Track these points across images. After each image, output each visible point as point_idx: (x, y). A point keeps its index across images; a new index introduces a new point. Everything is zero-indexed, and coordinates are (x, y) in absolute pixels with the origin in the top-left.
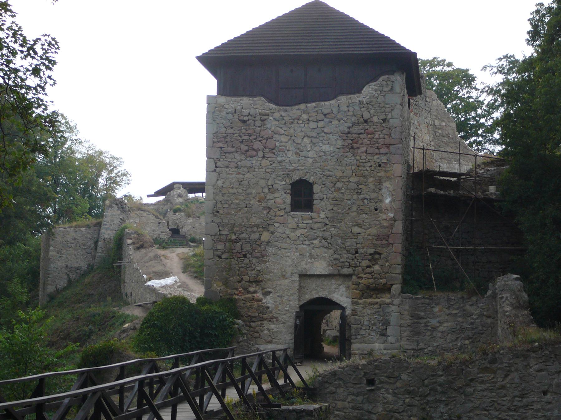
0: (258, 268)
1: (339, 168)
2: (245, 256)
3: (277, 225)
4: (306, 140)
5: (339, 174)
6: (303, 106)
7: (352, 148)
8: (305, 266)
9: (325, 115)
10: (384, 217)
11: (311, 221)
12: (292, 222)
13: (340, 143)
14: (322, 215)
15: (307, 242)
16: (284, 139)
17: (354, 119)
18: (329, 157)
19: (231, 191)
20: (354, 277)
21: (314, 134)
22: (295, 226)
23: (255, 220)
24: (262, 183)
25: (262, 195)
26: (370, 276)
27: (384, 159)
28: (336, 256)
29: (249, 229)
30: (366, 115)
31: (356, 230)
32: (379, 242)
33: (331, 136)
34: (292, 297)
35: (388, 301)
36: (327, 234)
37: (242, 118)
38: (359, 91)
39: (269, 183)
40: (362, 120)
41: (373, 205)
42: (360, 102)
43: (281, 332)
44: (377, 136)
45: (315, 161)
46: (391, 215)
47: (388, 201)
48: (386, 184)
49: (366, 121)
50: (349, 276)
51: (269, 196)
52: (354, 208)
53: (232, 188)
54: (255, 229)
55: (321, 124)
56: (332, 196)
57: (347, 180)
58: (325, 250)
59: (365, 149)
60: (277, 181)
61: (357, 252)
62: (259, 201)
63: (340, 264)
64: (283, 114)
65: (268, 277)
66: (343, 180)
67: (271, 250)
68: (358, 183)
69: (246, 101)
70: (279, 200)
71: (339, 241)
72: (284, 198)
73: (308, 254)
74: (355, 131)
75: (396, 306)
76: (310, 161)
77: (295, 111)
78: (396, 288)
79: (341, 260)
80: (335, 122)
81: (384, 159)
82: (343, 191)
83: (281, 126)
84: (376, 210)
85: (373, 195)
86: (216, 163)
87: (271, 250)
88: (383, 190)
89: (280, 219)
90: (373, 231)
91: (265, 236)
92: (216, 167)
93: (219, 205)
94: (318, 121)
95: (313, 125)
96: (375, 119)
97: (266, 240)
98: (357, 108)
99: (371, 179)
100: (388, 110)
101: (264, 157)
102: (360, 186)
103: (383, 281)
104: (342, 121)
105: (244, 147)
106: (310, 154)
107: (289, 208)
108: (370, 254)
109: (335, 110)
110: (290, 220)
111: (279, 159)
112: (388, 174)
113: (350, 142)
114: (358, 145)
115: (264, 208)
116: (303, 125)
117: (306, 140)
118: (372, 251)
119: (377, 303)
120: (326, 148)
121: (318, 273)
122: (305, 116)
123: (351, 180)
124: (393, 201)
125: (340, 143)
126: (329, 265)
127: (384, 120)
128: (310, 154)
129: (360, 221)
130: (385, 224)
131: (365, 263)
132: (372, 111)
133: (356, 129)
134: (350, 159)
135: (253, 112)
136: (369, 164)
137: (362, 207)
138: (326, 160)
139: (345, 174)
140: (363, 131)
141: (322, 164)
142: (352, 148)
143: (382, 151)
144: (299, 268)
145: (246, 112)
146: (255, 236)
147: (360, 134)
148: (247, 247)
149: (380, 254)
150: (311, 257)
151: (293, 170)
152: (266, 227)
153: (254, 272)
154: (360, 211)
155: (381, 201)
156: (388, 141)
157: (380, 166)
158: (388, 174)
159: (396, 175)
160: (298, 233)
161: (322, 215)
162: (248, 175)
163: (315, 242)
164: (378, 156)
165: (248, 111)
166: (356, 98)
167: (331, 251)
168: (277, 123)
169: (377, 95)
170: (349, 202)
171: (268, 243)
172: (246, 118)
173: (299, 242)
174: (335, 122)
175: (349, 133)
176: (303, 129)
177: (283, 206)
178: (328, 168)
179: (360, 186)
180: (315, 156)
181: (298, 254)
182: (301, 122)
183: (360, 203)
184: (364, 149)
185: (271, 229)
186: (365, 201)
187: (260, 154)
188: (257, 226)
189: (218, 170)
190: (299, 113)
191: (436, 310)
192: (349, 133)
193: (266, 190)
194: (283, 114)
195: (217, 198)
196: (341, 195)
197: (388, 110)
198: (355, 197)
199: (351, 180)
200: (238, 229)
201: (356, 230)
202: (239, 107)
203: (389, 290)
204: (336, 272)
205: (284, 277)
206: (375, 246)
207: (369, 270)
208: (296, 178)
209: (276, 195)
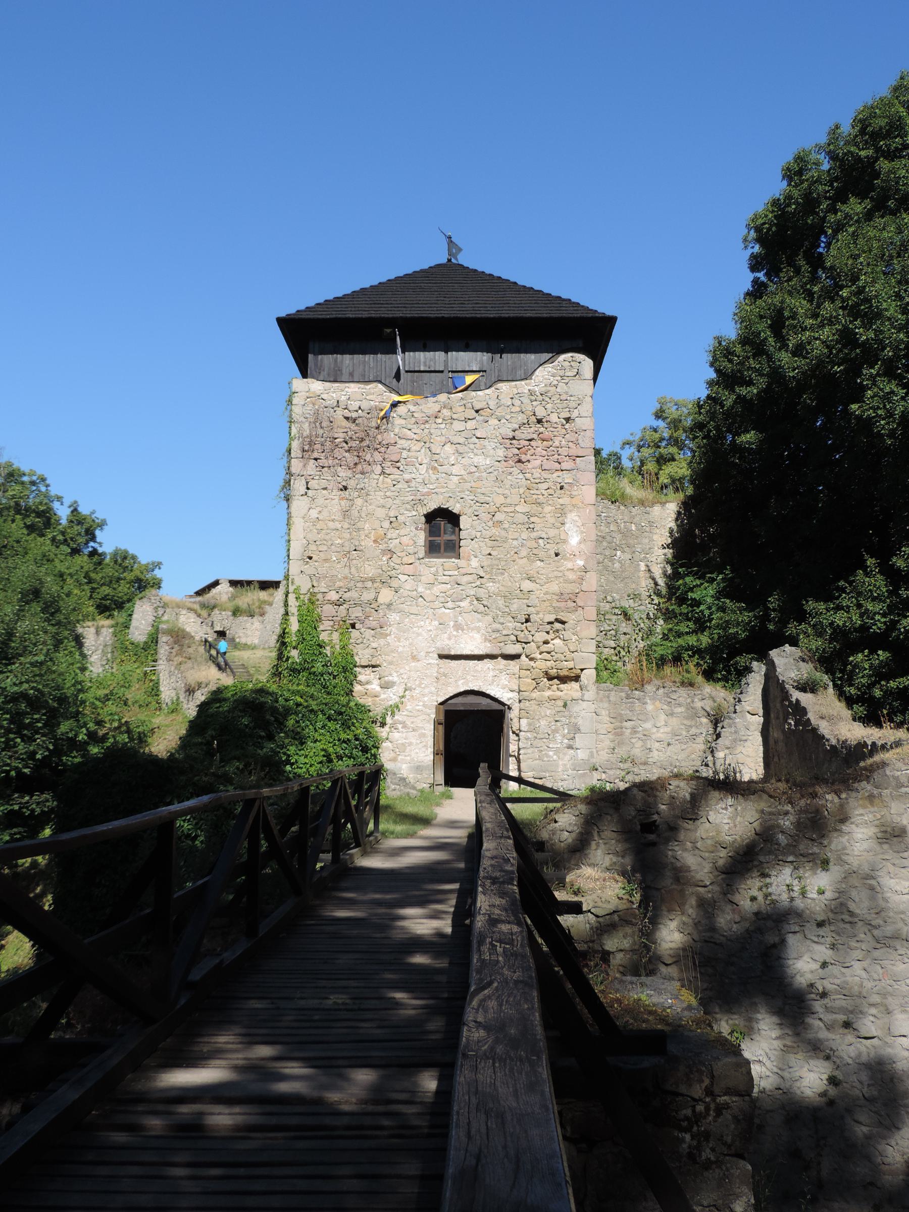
0: (374, 645)
1: (500, 491)
2: (353, 626)
3: (403, 578)
4: (448, 448)
5: (500, 500)
6: (443, 397)
7: (520, 461)
8: (447, 642)
9: (477, 411)
10: (570, 565)
11: (456, 573)
12: (427, 576)
13: (501, 453)
14: (474, 563)
15: (450, 605)
16: (416, 447)
17: (522, 418)
18: (484, 474)
19: (331, 524)
20: (523, 657)
21: (462, 440)
22: (431, 578)
23: (370, 570)
24: (380, 513)
25: (381, 532)
26: (548, 656)
27: (567, 478)
28: (496, 626)
29: (359, 585)
30: (541, 413)
31: (527, 585)
32: (562, 604)
33: (486, 443)
34: (426, 691)
35: (577, 694)
36: (481, 593)
37: (348, 414)
38: (527, 377)
39: (392, 514)
40: (533, 419)
41: (553, 549)
42: (531, 393)
43: (410, 744)
44: (557, 443)
45: (463, 480)
46: (581, 563)
47: (574, 540)
48: (572, 516)
49: (539, 421)
50: (516, 657)
51: (392, 534)
52: (524, 553)
53: (333, 520)
54: (369, 584)
55: (471, 424)
56: (488, 534)
57: (511, 509)
58: (479, 616)
59: (538, 462)
60: (402, 511)
61: (527, 621)
62: (375, 541)
63: (503, 638)
64: (412, 408)
65: (390, 658)
66: (506, 509)
67: (394, 617)
68: (528, 515)
69: (353, 388)
70: (405, 540)
71: (501, 602)
72: (416, 536)
73: (452, 624)
74: (523, 436)
75: (588, 703)
76: (455, 479)
77: (430, 405)
78: (589, 676)
79: (505, 632)
80: (493, 422)
81: (567, 478)
82: (506, 526)
83: (409, 426)
84: (557, 555)
85: (552, 533)
86: (307, 483)
87: (394, 617)
88: (567, 526)
89: (409, 569)
90: (554, 587)
91: (385, 596)
92: (308, 489)
93: (313, 547)
94: (466, 420)
95: (458, 426)
96: (554, 418)
97: (387, 601)
98: (526, 400)
99: (548, 509)
100: (573, 404)
101: (383, 473)
102: (532, 519)
103: (570, 664)
104: (503, 421)
105: (351, 458)
106: (455, 470)
107: (422, 553)
108: (549, 623)
109: (492, 404)
110: (422, 569)
111: (407, 476)
112: (574, 501)
113: (517, 451)
114: (528, 457)
115: (384, 552)
116: (443, 426)
117: (448, 448)
118: (552, 618)
119: (559, 698)
120: (480, 460)
121: (469, 653)
122: (446, 412)
123: (518, 508)
124: (583, 541)
125: (501, 453)
126: (486, 640)
127: (568, 420)
128: (455, 470)
129: (532, 573)
130: (571, 576)
131: (541, 637)
132: (549, 406)
133: (527, 433)
134: (516, 476)
135: (365, 405)
136: (545, 486)
137: (535, 551)
138: (480, 479)
139: (508, 501)
140: (535, 436)
141: (473, 484)
142: (520, 461)
143: (565, 466)
144: (438, 644)
145: (354, 405)
146: (368, 596)
147: (530, 440)
148: (356, 613)
149: (563, 623)
150: (458, 627)
151: (428, 494)
152: (385, 580)
153: (367, 651)
154: (533, 556)
155: (565, 541)
156: (574, 451)
157: (562, 488)
158: (574, 501)
159: (586, 502)
160: (437, 589)
161: (474, 563)
162: (359, 502)
163: (462, 604)
164: (560, 473)
165: (357, 404)
166: (524, 386)
167: (489, 618)
168: (403, 422)
169: (555, 382)
170: (515, 542)
171: (389, 605)
172: (354, 415)
173: (437, 604)
174: (493, 422)
175: (514, 438)
176: (444, 432)
177: (411, 549)
178: (483, 490)
179: (532, 519)
180: (463, 472)
181: (436, 623)
182: (439, 421)
183: (533, 544)
184: (538, 463)
185: (395, 583)
186: (541, 541)
187: (378, 469)
188: (373, 580)
189: (310, 493)
190: (437, 407)
191: (650, 707)
192: (514, 438)
193: (386, 524)
194: (412, 408)
195: (309, 536)
196: (503, 533)
197: (573, 404)
198: (525, 535)
199: (518, 508)
200: (341, 584)
201: (527, 585)
202: (343, 398)
203: (577, 678)
204: (496, 652)
205: (414, 658)
206: (556, 610)
207: (545, 648)
208: (432, 506)
209: (402, 532)
